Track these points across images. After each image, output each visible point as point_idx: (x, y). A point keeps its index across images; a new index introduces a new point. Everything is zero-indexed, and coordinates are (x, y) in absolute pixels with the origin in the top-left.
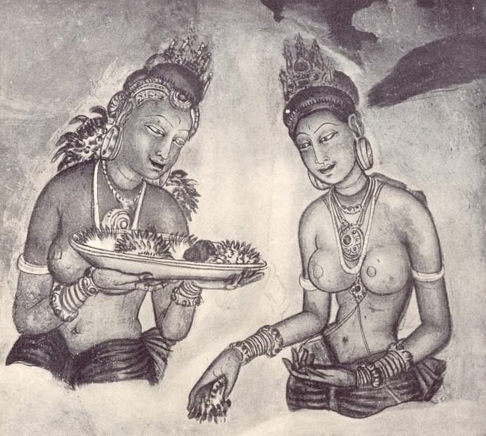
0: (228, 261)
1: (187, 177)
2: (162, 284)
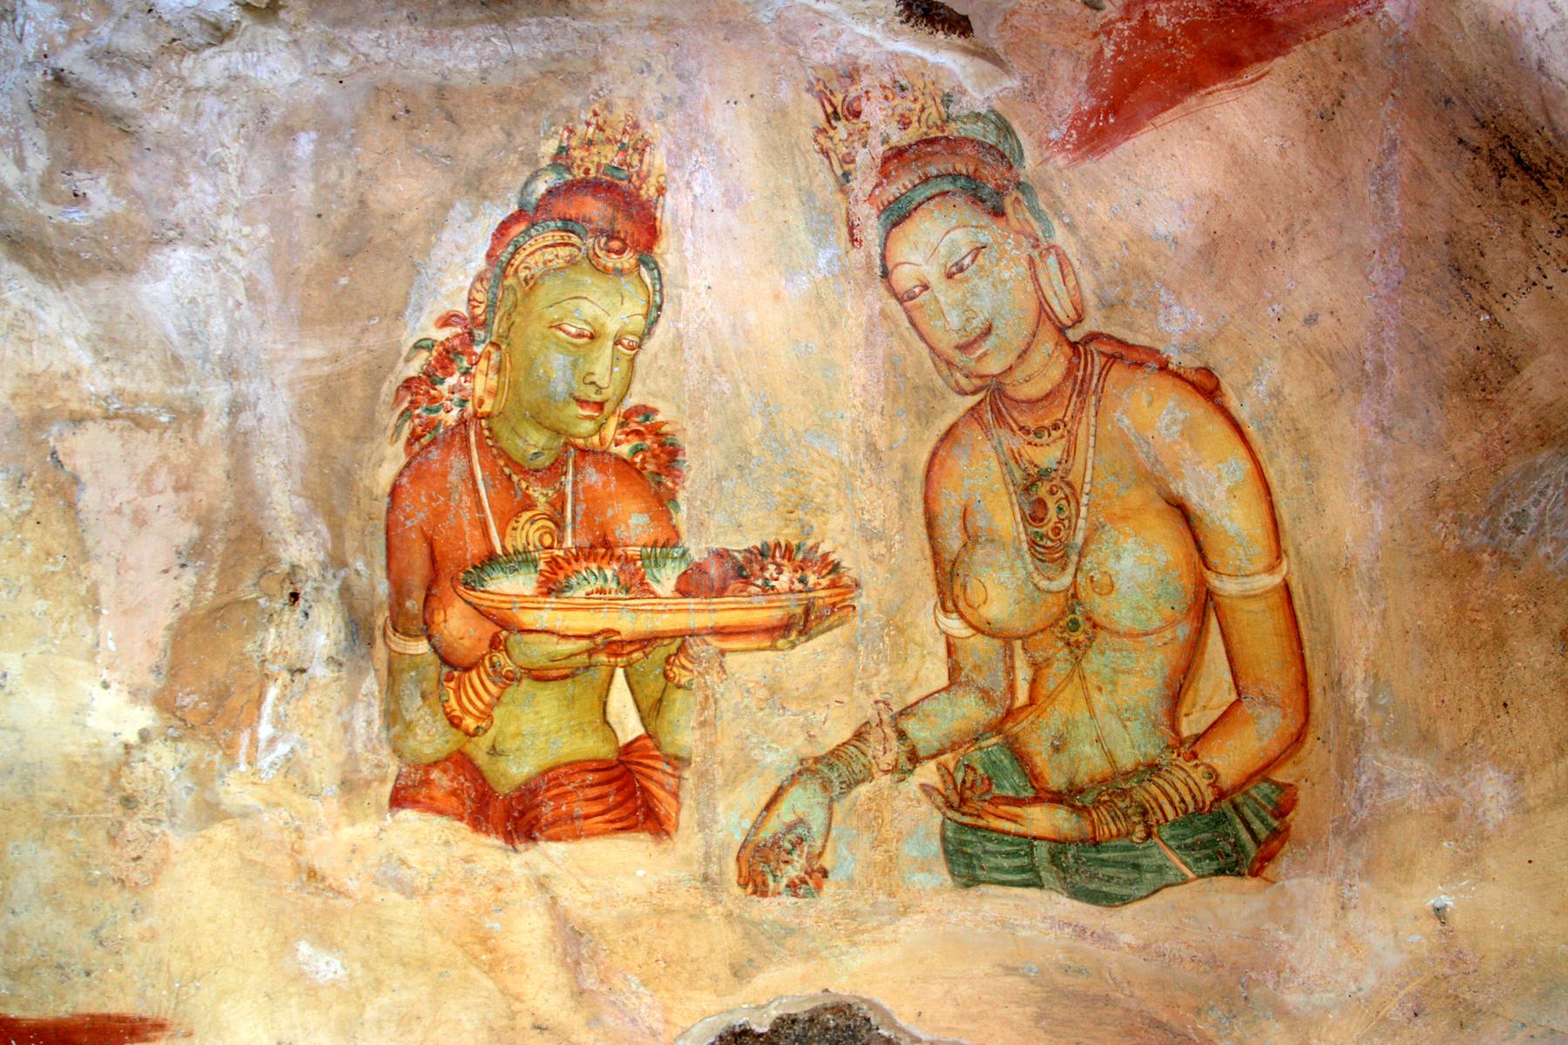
0: (773, 588)
1: (659, 418)
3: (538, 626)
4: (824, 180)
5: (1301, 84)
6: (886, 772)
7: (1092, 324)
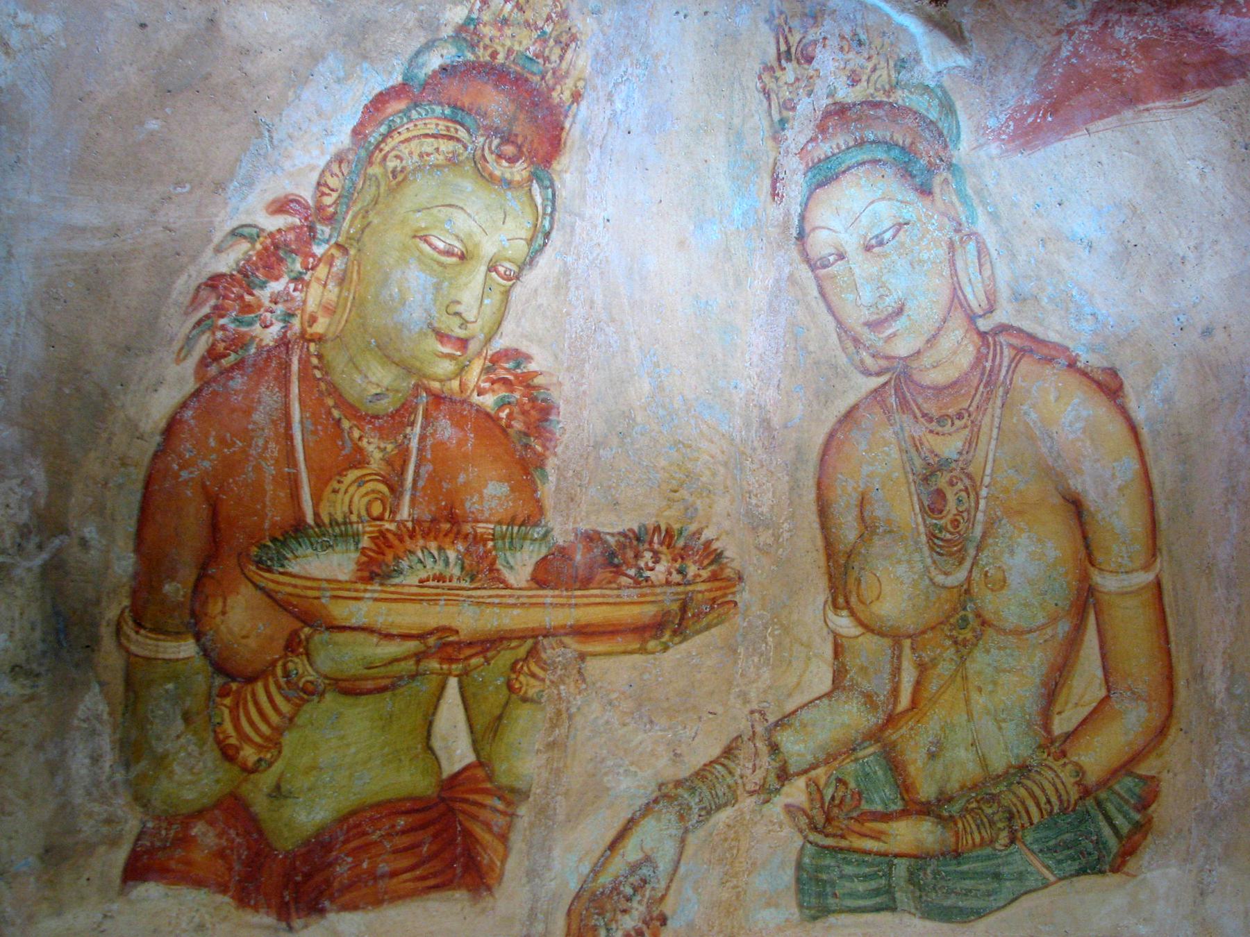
0: (647, 579)
1: (533, 367)
2: (483, 652)
3: (353, 622)
4: (758, 121)
5: (1233, 115)
6: (751, 793)
7: (1005, 314)
